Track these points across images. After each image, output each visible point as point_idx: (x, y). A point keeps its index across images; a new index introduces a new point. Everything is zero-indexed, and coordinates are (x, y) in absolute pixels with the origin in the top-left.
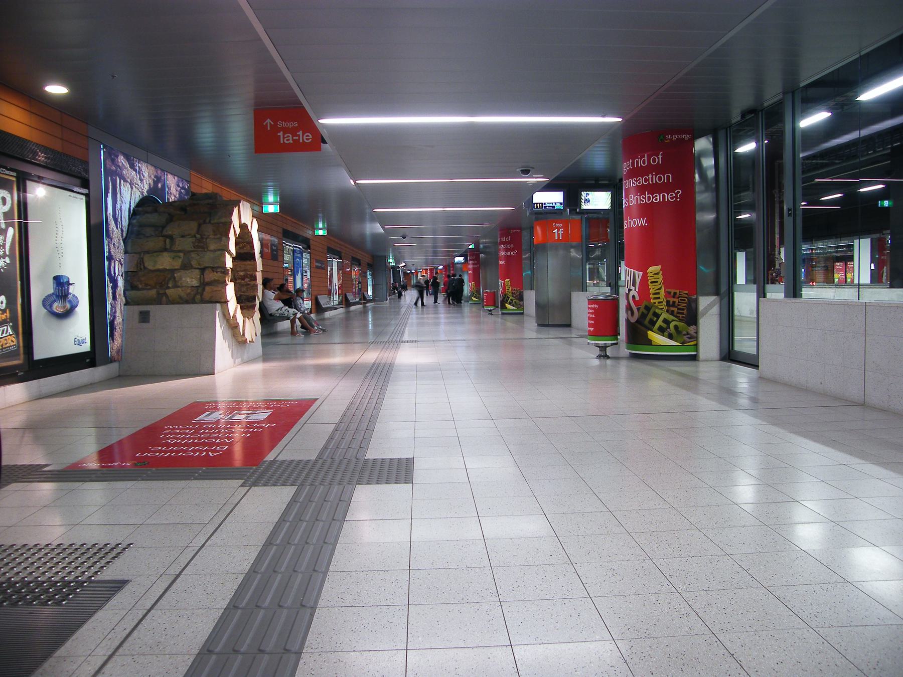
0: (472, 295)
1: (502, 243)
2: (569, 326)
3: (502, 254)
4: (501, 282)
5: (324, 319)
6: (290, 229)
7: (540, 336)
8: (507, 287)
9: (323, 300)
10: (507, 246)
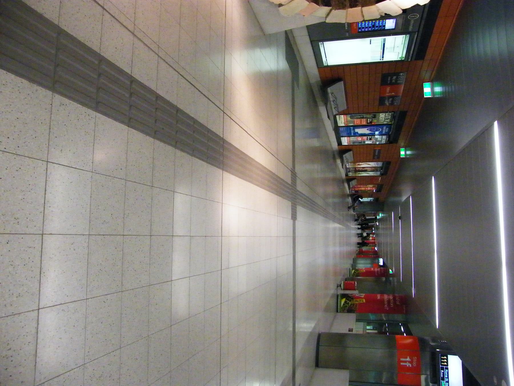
0: (357, 270)
1: (394, 298)
2: (317, 365)
3: (386, 297)
4: (363, 295)
5: (334, 158)
6: (408, 119)
7: (299, 347)
8: (358, 300)
9: (348, 156)
10: (392, 301)
